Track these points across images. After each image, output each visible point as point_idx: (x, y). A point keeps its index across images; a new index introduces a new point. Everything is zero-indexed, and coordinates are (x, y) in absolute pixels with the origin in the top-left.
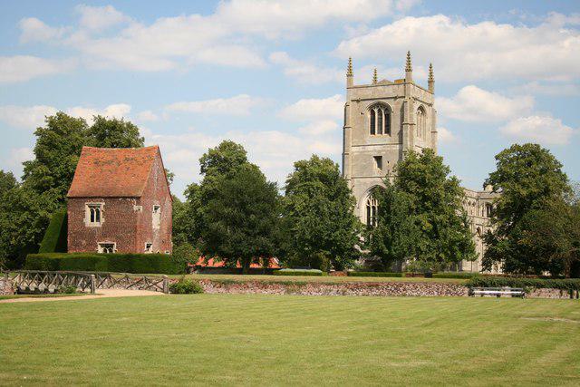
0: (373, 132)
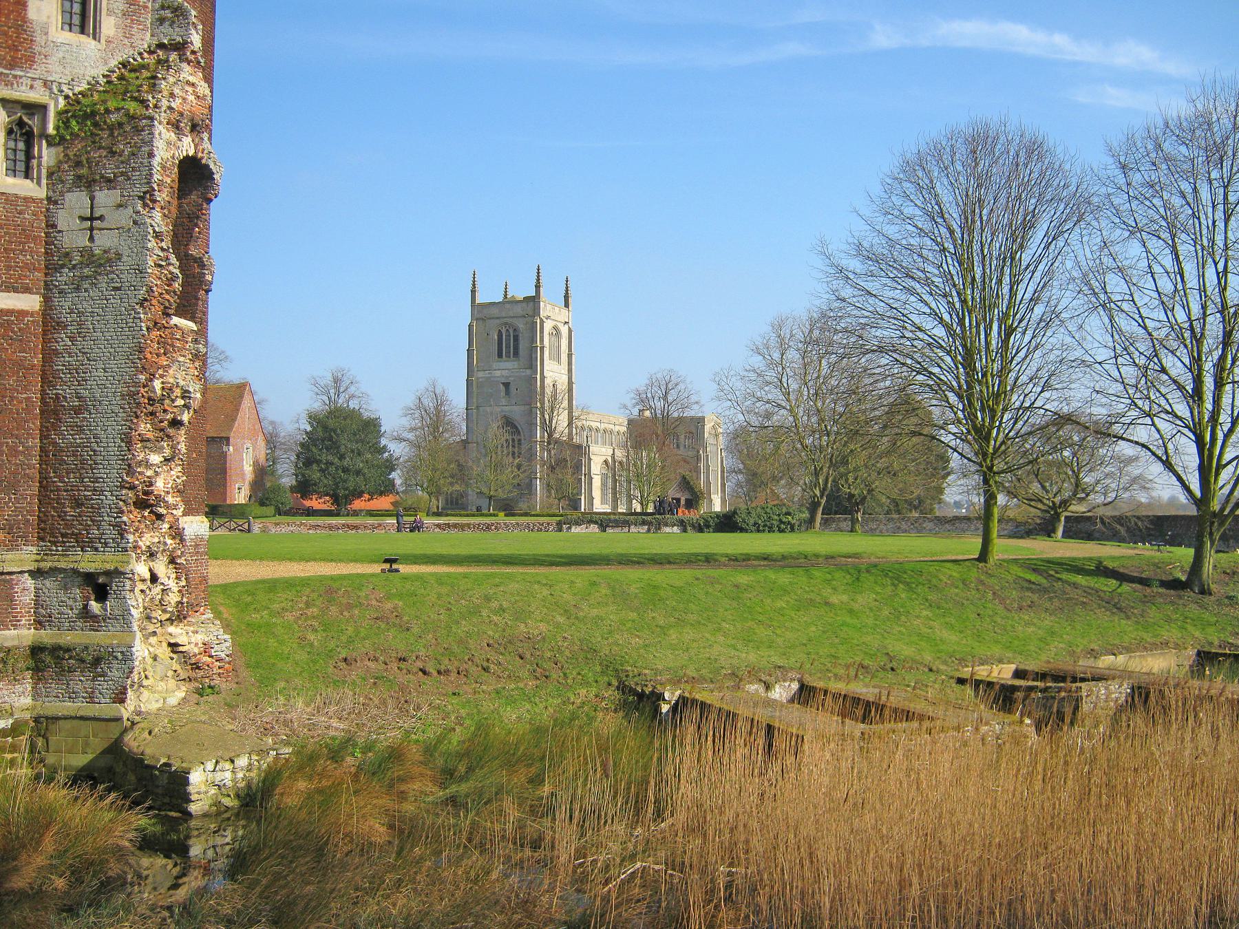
0: (500, 355)
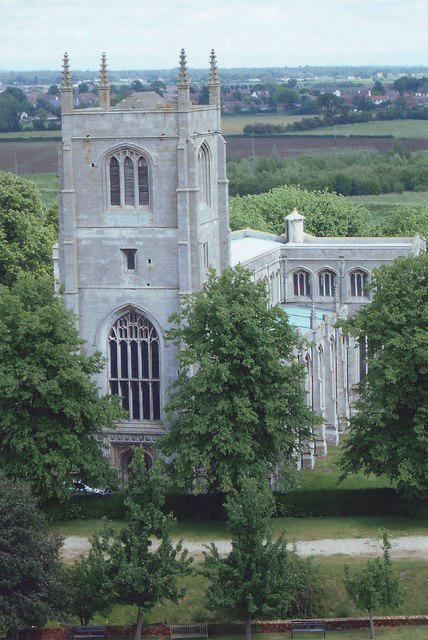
0: (116, 200)
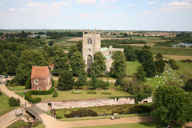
0: (88, 44)
